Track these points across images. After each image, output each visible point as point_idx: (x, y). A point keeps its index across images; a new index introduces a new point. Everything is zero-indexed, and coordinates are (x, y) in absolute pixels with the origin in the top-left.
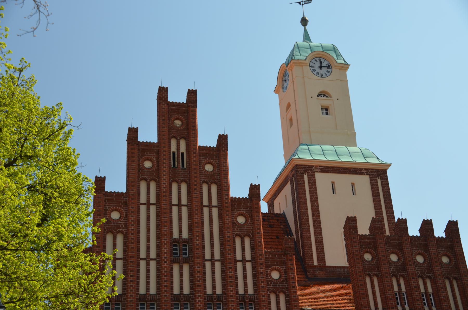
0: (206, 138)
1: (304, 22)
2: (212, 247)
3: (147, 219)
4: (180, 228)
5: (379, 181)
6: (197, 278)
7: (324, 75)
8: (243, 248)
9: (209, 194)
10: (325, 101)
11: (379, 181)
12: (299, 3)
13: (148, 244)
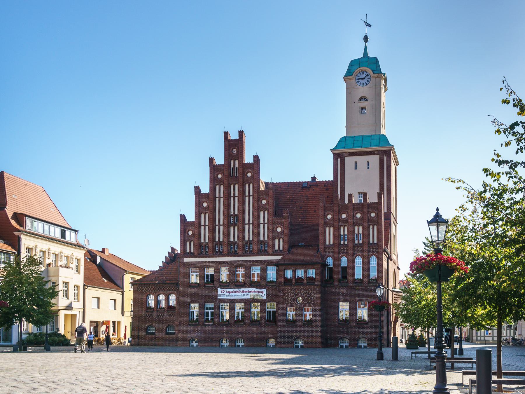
0: (248, 159)
1: (366, 39)
2: (249, 217)
3: (220, 205)
4: (234, 209)
5: (385, 158)
6: (242, 233)
7: (365, 84)
8: (264, 216)
9: (249, 189)
10: (363, 104)
11: (385, 158)
13: (220, 218)
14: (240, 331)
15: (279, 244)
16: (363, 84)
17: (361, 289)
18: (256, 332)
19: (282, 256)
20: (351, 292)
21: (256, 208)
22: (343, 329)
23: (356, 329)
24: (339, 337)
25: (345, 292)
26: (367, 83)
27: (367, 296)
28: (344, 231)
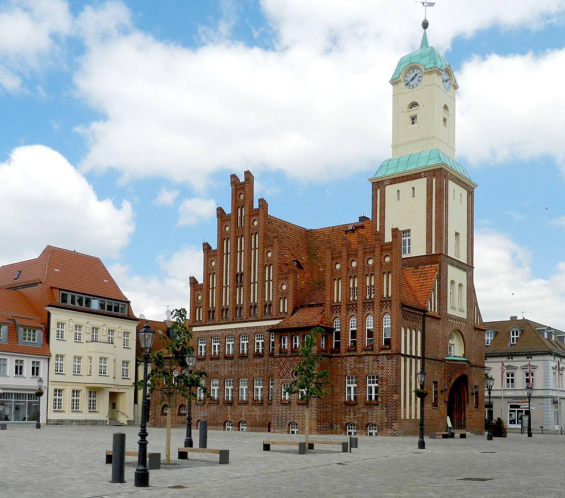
1: (425, 25)
7: (415, 86)
12: (423, 3)
14: (243, 413)
15: (285, 306)
16: (413, 86)
17: (371, 358)
18: (258, 413)
19: (281, 320)
20: (360, 363)
21: (261, 263)
22: (350, 411)
23: (365, 411)
24: (345, 421)
25: (353, 363)
26: (418, 83)
27: (378, 367)
28: (354, 283)
